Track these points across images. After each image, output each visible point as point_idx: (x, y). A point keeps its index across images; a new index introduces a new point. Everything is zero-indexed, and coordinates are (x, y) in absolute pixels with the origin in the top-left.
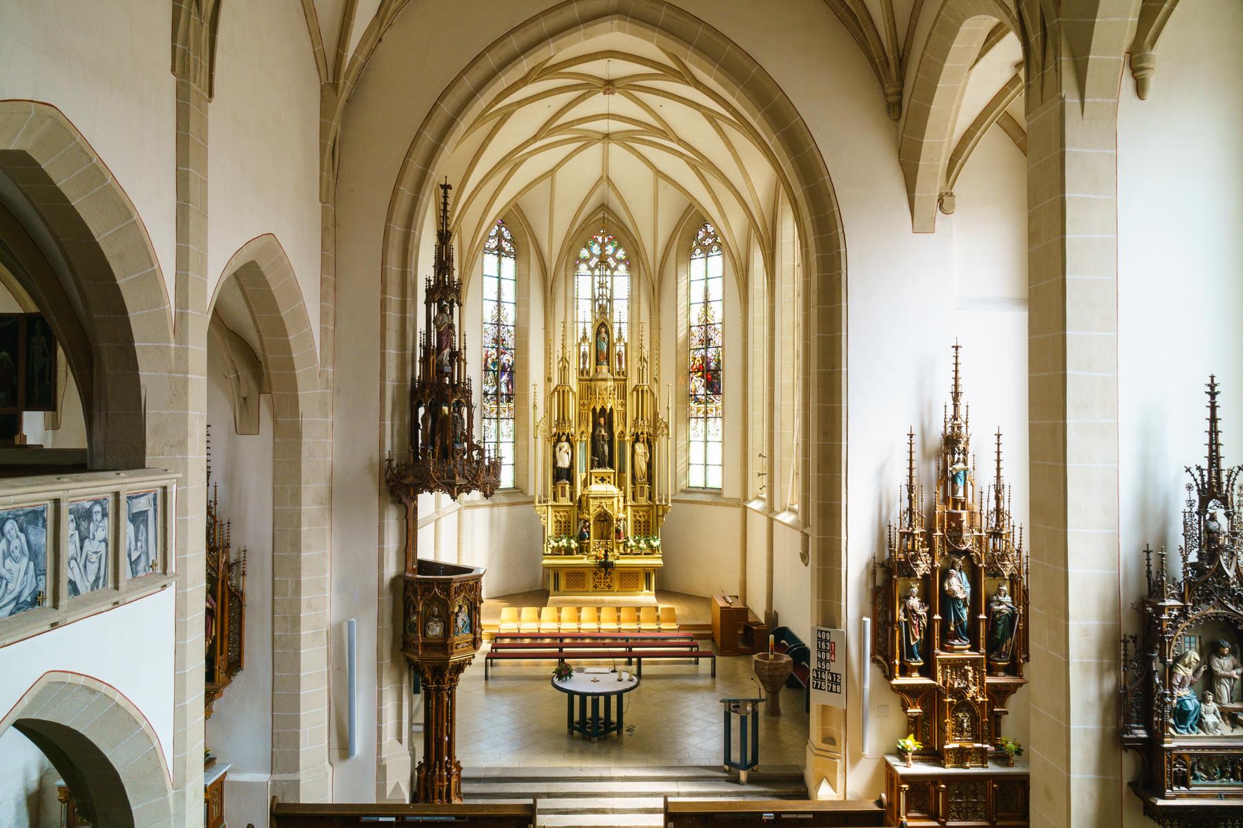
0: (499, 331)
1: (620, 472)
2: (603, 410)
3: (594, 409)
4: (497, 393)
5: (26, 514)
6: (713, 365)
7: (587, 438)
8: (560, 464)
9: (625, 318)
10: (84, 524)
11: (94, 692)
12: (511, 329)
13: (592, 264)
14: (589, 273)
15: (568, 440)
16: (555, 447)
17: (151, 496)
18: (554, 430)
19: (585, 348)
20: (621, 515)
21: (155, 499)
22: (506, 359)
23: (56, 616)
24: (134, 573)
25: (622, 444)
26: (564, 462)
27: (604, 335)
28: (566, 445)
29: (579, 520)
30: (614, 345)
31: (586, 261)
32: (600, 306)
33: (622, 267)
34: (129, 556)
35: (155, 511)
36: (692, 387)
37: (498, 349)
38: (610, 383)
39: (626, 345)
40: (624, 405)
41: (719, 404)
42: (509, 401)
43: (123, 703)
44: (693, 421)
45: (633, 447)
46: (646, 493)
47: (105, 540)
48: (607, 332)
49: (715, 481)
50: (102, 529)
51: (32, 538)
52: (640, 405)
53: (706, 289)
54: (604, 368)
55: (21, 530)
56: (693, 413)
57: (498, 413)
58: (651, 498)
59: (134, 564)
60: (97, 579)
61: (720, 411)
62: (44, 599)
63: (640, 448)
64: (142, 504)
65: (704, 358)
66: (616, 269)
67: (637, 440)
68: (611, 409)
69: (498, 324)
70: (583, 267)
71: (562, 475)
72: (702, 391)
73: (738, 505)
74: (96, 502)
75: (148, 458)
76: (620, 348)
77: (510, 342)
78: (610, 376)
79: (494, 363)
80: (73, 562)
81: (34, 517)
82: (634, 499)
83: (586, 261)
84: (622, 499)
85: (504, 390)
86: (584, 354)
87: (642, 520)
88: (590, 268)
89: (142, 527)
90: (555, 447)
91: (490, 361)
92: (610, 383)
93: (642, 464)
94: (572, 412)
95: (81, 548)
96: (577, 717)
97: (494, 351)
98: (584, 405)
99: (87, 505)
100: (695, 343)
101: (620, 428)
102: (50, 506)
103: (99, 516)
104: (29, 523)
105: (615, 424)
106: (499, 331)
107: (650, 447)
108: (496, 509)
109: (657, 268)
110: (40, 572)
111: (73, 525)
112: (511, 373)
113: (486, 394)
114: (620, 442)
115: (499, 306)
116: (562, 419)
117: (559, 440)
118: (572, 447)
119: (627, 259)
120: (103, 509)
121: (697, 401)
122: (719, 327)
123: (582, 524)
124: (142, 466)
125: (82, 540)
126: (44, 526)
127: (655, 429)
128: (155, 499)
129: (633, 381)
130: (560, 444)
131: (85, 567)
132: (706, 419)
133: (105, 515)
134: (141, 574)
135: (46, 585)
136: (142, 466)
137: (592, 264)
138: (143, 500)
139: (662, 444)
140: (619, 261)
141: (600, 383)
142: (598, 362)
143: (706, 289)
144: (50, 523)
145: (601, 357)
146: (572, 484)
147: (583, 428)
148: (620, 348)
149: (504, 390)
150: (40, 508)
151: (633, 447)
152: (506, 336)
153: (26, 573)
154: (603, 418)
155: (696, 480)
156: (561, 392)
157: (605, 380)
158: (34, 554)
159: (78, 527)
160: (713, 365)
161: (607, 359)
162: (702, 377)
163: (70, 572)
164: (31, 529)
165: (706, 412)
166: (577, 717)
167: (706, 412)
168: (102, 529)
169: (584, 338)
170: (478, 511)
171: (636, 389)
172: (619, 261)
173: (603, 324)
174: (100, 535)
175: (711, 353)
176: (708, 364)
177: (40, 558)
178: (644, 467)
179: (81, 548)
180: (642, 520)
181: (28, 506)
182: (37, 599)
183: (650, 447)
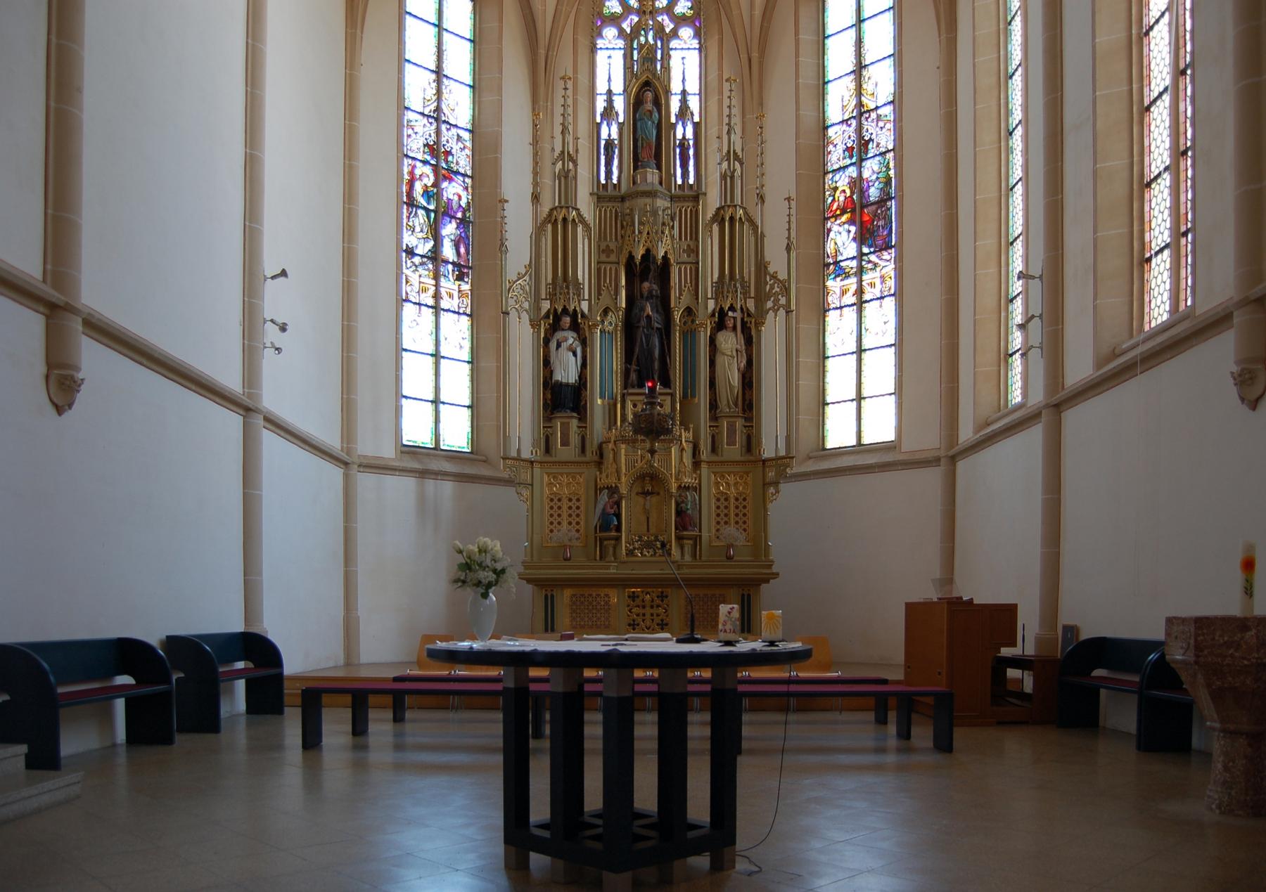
0: (438, 132)
1: (685, 396)
2: (648, 255)
3: (631, 257)
4: (435, 256)
6: (874, 193)
7: (614, 321)
8: (559, 376)
9: (693, 86)
12: (466, 136)
13: (626, 26)
14: (621, 43)
15: (575, 327)
16: (547, 341)
18: (546, 306)
19: (610, 131)
20: (687, 480)
22: (454, 191)
25: (690, 336)
26: (567, 371)
27: (649, 106)
28: (571, 338)
29: (598, 490)
30: (674, 126)
31: (615, 20)
32: (641, 47)
33: (686, 32)
36: (830, 248)
37: (436, 168)
38: (661, 203)
39: (696, 126)
40: (693, 251)
41: (890, 269)
42: (460, 278)
44: (832, 317)
45: (712, 341)
46: (739, 438)
48: (656, 102)
49: (881, 426)
52: (730, 250)
53: (859, 42)
54: (652, 176)
56: (833, 300)
57: (437, 296)
58: (751, 444)
61: (891, 283)
63: (729, 342)
65: (858, 184)
66: (675, 34)
67: (720, 325)
68: (665, 258)
69: (437, 117)
70: (610, 32)
71: (561, 400)
72: (850, 249)
73: (935, 461)
76: (684, 132)
77: (462, 160)
78: (662, 189)
79: (426, 193)
82: (714, 450)
83: (615, 20)
84: (688, 448)
85: (448, 252)
86: (609, 143)
87: (733, 492)
88: (621, 33)
90: (547, 341)
91: (418, 187)
92: (661, 203)
93: (731, 374)
94: (583, 272)
96: (540, 810)
97: (428, 170)
98: (607, 251)
100: (836, 157)
101: (686, 300)
105: (674, 294)
106: (438, 132)
107: (749, 341)
108: (430, 484)
109: (758, 13)
112: (463, 223)
113: (410, 252)
114: (684, 334)
115: (439, 82)
116: (564, 281)
117: (555, 327)
118: (584, 343)
119: (697, 16)
121: (842, 273)
122: (887, 111)
123: (604, 498)
127: (760, 299)
129: (713, 200)
130: (559, 335)
132: (860, 304)
137: (626, 26)
139: (772, 332)
140: (680, 21)
141: (641, 201)
142: (637, 162)
143: (859, 42)
145: (643, 155)
146: (582, 418)
147: (606, 300)
148: (684, 132)
149: (448, 252)
151: (712, 341)
152: (455, 147)
154: (648, 274)
155: (839, 434)
156: (556, 223)
157: (652, 194)
160: (874, 193)
161: (658, 156)
162: (851, 222)
165: (860, 291)
166: (540, 810)
167: (860, 291)
169: (609, 112)
170: (391, 481)
171: (718, 218)
172: (680, 21)
173: (647, 84)
175: (871, 168)
176: (863, 193)
178: (736, 379)
180: (733, 492)
183: (749, 341)
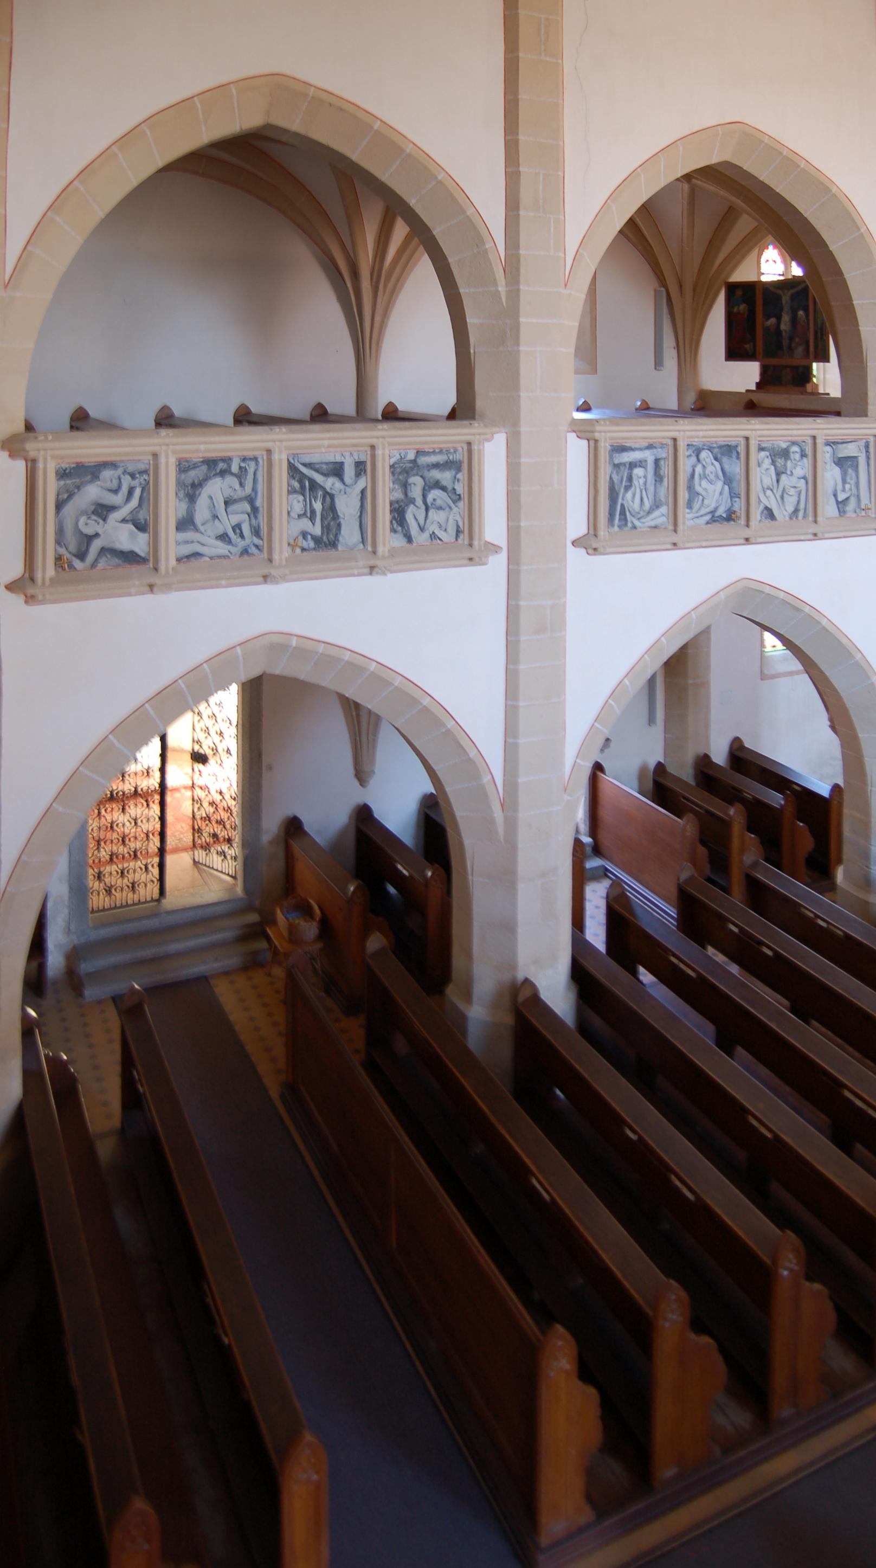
5: (720, 447)
10: (780, 462)
11: (797, 609)
17: (862, 443)
21: (867, 446)
23: (747, 533)
24: (842, 512)
34: (835, 495)
35: (868, 458)
43: (830, 628)
47: (804, 478)
50: (801, 468)
51: (726, 467)
55: (716, 459)
59: (841, 505)
60: (796, 511)
62: (739, 518)
64: (850, 450)
74: (794, 443)
75: (870, 407)
80: (769, 493)
81: (728, 450)
89: (850, 471)
95: (778, 481)
99: (784, 445)
102: (743, 442)
103: (798, 456)
104: (723, 454)
110: (733, 495)
111: (767, 462)
120: (802, 451)
124: (866, 415)
125: (778, 474)
126: (738, 458)
128: (867, 446)
131: (782, 497)
133: (803, 455)
134: (850, 514)
135: (739, 506)
136: (865, 414)
138: (850, 446)
144: (743, 456)
150: (733, 444)
153: (721, 493)
158: (728, 480)
159: (773, 463)
163: (762, 497)
164: (725, 459)
168: (801, 468)
174: (799, 472)
177: (735, 484)
179: (778, 481)
181: (722, 441)
182: (730, 517)
